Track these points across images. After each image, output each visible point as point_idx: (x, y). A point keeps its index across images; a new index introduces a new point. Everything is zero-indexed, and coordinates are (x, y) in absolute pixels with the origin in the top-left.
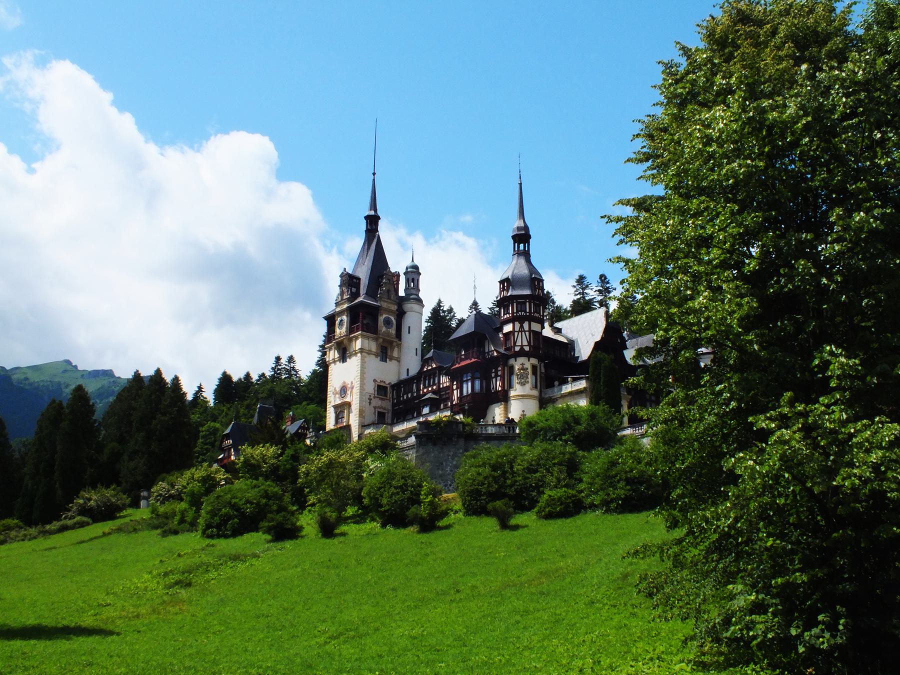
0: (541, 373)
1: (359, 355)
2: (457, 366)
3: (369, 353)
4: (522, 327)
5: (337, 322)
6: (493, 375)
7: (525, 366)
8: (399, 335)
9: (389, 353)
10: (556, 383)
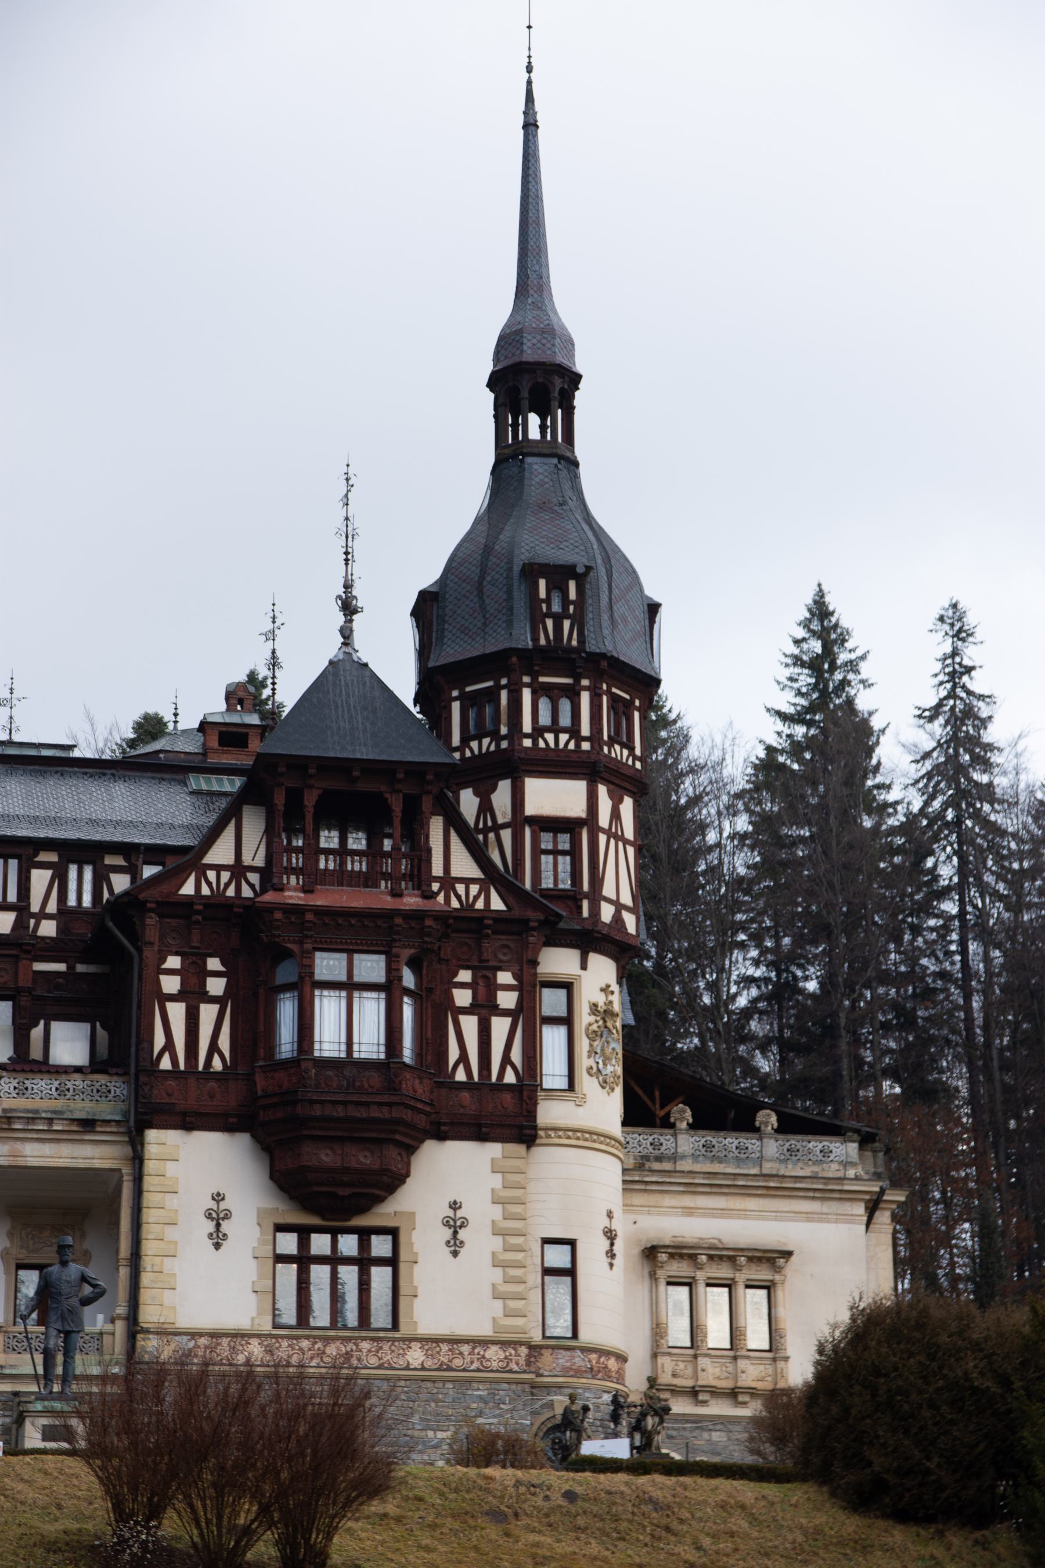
2: (293, 896)
4: (616, 815)
6: (463, 998)
10: (683, 1114)
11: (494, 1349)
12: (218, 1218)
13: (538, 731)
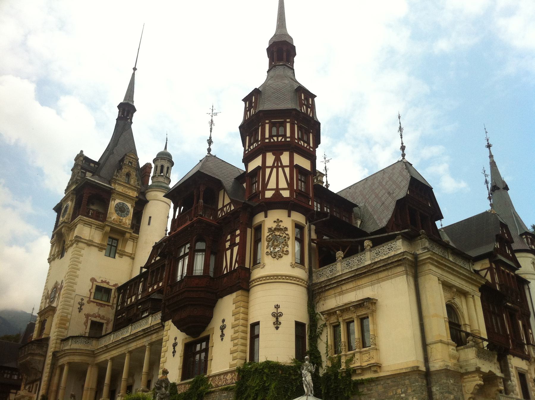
0: (311, 240)
1: (75, 245)
3: (90, 244)
4: (278, 159)
5: (63, 211)
6: (228, 244)
7: (282, 225)
8: (136, 226)
9: (119, 248)
10: (340, 254)
11: (229, 375)
12: (175, 345)
13: (249, 147)
